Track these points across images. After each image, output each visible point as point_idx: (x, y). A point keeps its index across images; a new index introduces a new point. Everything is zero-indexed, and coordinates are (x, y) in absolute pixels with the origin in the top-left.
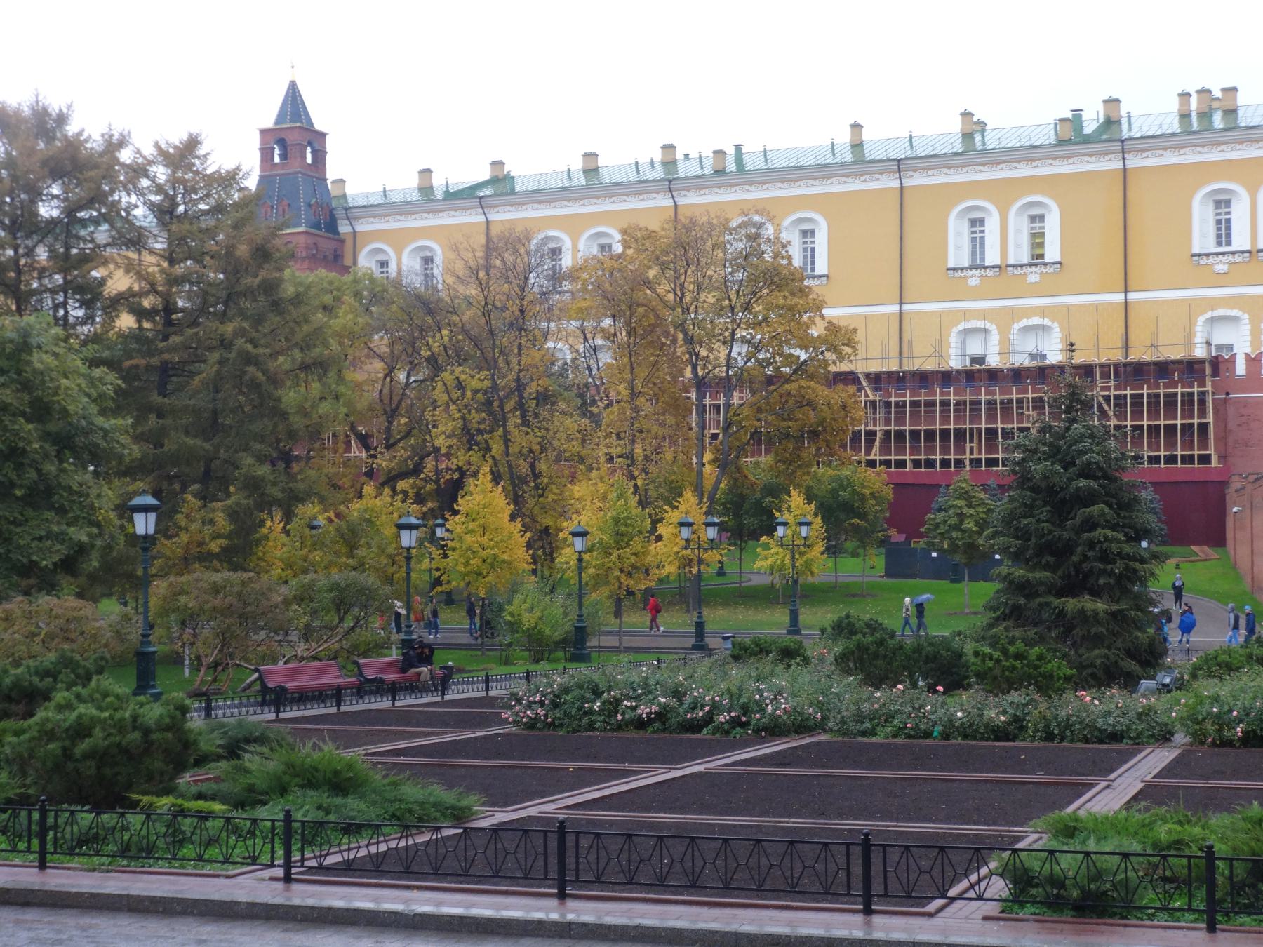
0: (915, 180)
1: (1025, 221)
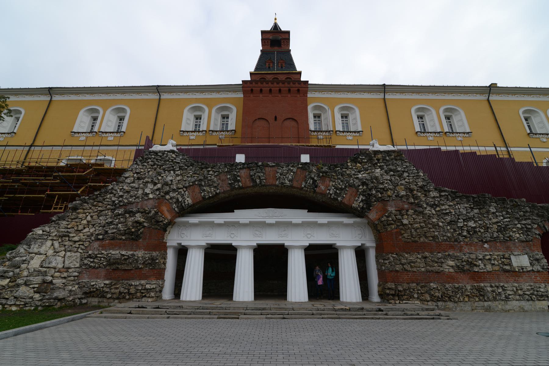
0: (165, 96)
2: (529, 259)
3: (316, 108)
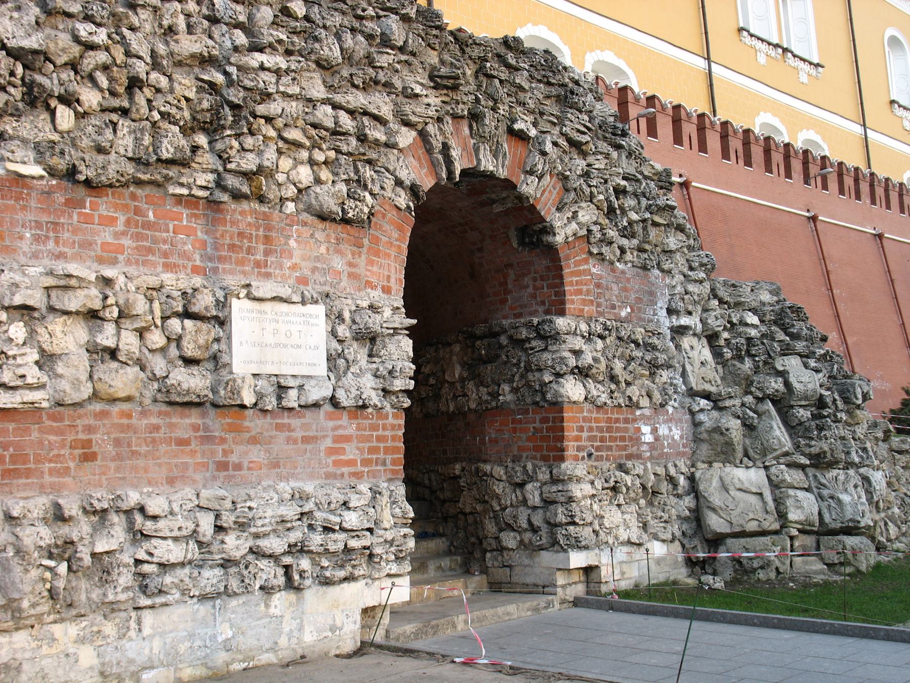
2: (333, 333)
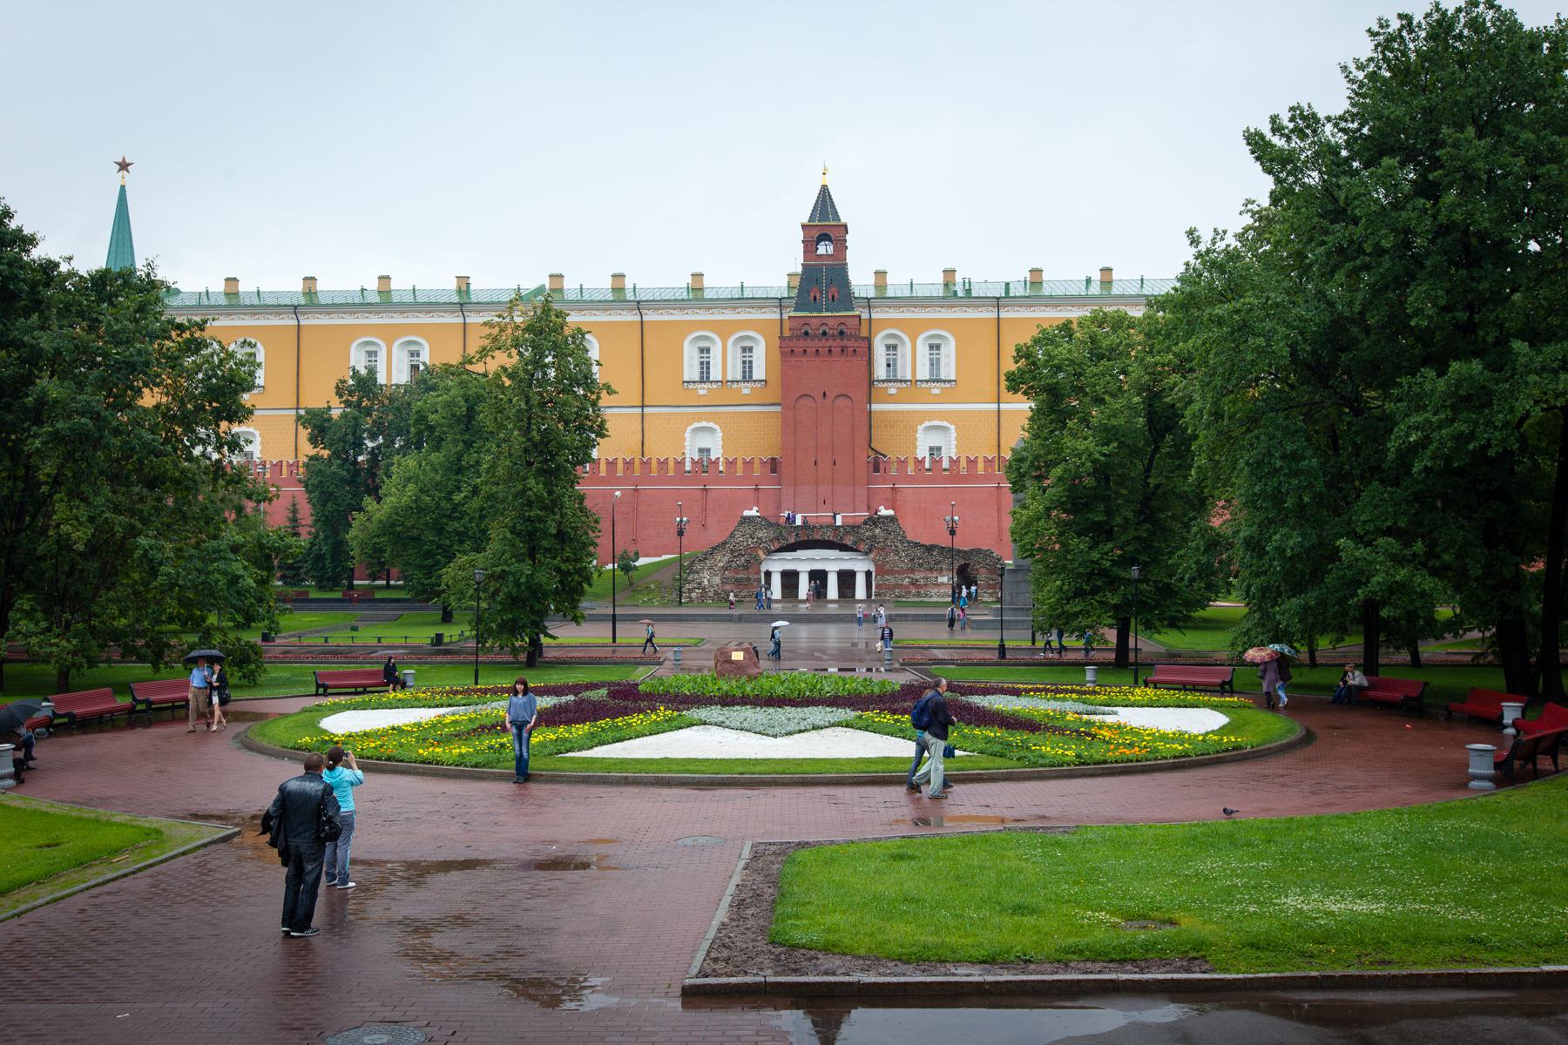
0: (650, 317)
1: (696, 354)
3: (889, 336)
